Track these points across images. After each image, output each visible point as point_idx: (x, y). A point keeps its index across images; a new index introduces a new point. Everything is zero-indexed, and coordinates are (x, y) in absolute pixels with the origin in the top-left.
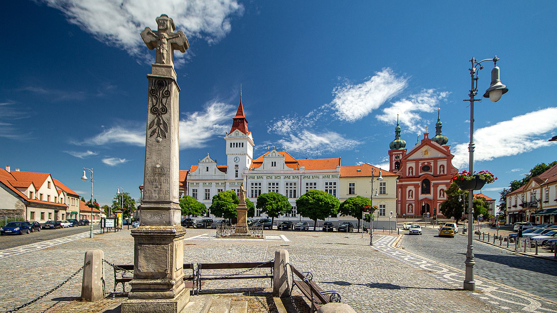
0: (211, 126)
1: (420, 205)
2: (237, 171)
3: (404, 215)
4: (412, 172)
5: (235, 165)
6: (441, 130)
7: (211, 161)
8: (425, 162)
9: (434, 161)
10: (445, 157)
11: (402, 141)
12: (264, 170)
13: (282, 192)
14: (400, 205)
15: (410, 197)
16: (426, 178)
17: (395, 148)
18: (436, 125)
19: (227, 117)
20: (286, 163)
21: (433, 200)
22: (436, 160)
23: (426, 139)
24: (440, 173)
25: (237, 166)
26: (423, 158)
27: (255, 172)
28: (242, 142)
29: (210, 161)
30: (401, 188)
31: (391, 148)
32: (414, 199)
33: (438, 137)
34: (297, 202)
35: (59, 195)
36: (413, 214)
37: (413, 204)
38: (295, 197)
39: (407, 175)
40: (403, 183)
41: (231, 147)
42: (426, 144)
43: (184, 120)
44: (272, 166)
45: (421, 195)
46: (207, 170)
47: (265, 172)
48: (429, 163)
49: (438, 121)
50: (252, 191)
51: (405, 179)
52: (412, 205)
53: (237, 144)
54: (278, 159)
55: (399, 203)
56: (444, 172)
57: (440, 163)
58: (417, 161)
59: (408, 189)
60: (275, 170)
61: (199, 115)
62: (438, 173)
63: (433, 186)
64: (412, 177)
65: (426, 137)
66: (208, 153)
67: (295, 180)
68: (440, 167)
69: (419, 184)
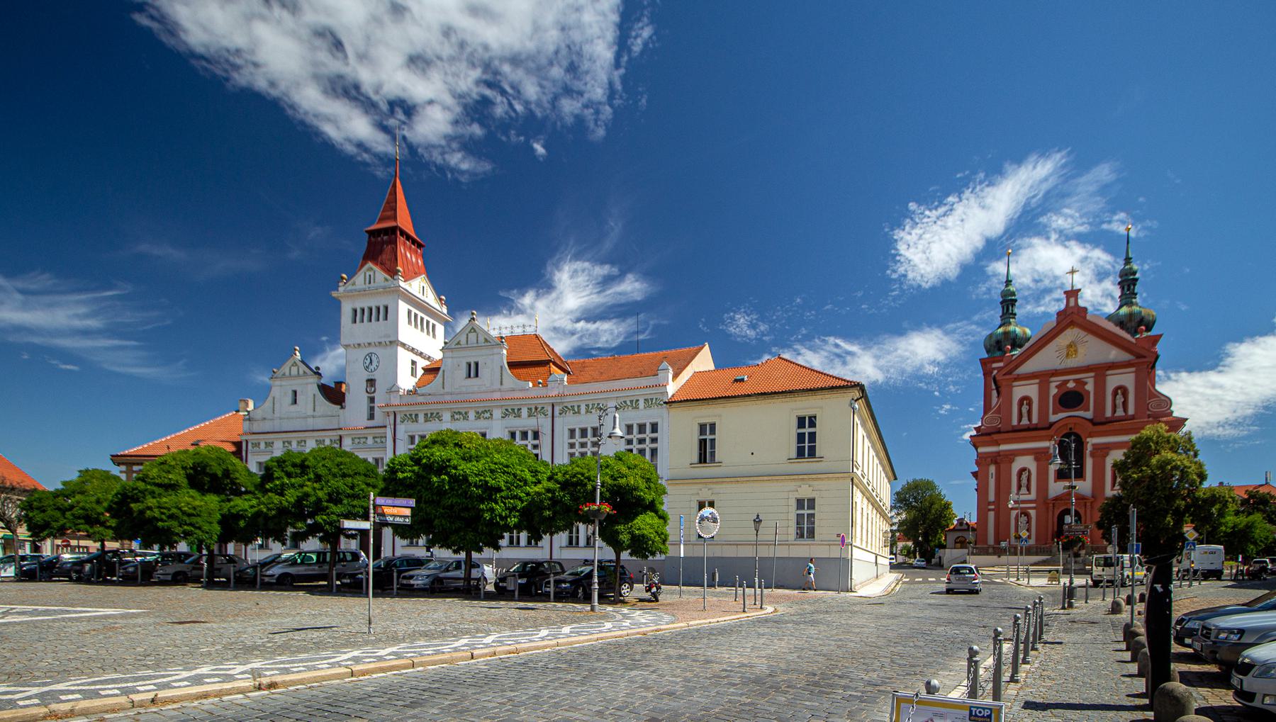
0: (569, 326)
1: (1051, 513)
2: (372, 400)
3: (1003, 544)
4: (1029, 412)
5: (368, 381)
6: (1136, 291)
7: (304, 372)
8: (1068, 381)
9: (1095, 377)
10: (1129, 361)
11: (1018, 330)
12: (446, 390)
14: (991, 515)
15: (1024, 490)
16: (1071, 429)
17: (1000, 349)
18: (1121, 276)
19: (597, 299)
20: (512, 365)
21: (1093, 497)
22: (1101, 370)
23: (1072, 307)
24: (1114, 411)
25: (371, 382)
26: (1063, 366)
27: (421, 399)
29: (301, 372)
30: (996, 463)
31: (988, 352)
32: (1033, 496)
33: (1125, 310)
36: (1032, 542)
37: (1033, 513)
39: (1015, 422)
40: (1003, 447)
42: (1072, 324)
43: (505, 312)
45: (1055, 482)
47: (448, 398)
48: (1081, 383)
49: (1126, 264)
51: (1006, 436)
52: (1027, 515)
54: (484, 352)
55: (990, 510)
56: (1125, 409)
57: (1113, 381)
58: (1043, 377)
59: (1016, 467)
60: (476, 389)
61: (538, 296)
62: (1108, 413)
63: (1092, 455)
64: (1028, 429)
65: (1072, 303)
66: (297, 348)
68: (1115, 393)
69: (1048, 448)
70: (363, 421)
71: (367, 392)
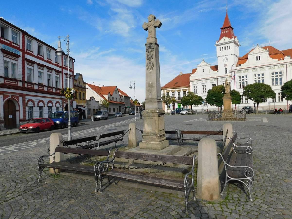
2: (226, 69)
13: (268, 82)
25: (226, 65)
28: (230, 45)
34: (283, 88)
35: (121, 98)
38: (281, 83)
41: (221, 51)
44: (257, 60)
46: (204, 71)
50: (240, 82)
53: (225, 47)
67: (281, 69)
70: (224, 74)
71: (225, 67)
